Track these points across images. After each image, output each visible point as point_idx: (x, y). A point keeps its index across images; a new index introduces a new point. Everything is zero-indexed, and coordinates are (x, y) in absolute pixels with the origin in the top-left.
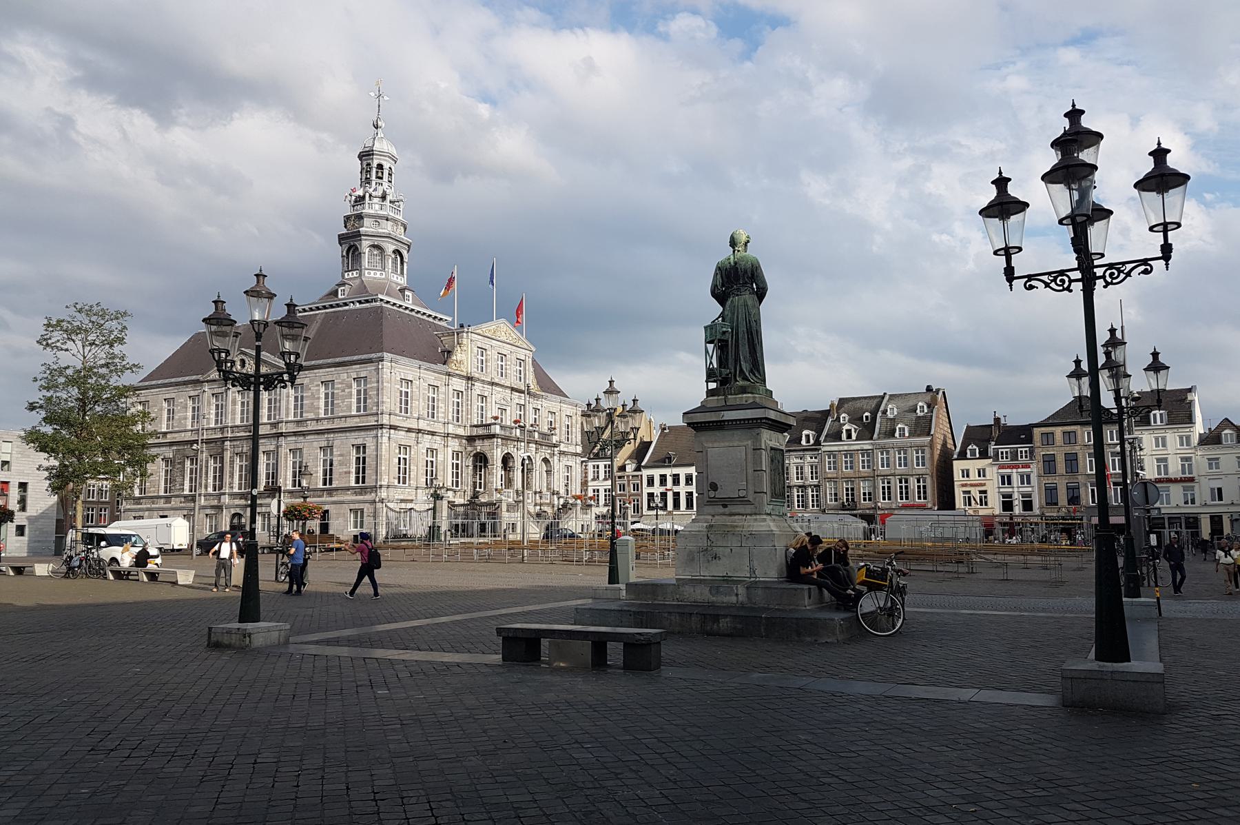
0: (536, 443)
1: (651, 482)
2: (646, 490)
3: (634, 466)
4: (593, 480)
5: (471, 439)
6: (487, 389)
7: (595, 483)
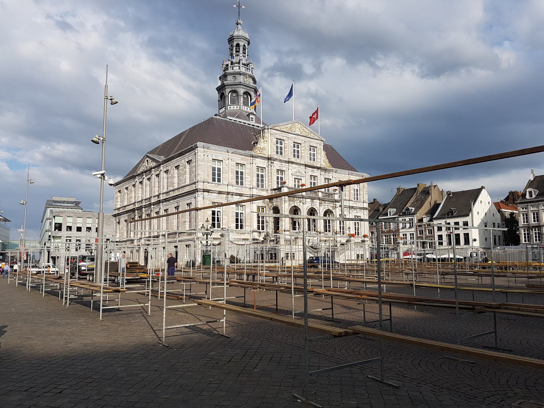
0: (319, 199)
1: (440, 229)
2: (437, 233)
3: (428, 218)
4: (403, 228)
5: (271, 198)
6: (284, 167)
7: (404, 230)
